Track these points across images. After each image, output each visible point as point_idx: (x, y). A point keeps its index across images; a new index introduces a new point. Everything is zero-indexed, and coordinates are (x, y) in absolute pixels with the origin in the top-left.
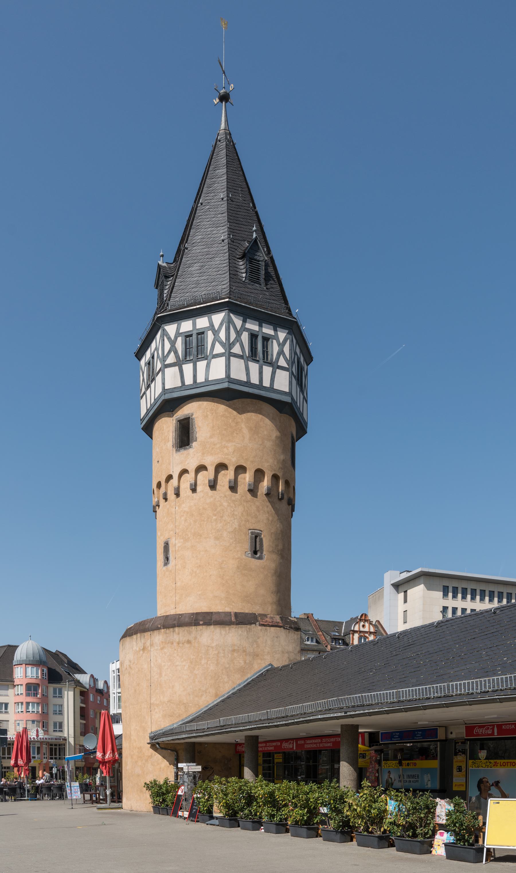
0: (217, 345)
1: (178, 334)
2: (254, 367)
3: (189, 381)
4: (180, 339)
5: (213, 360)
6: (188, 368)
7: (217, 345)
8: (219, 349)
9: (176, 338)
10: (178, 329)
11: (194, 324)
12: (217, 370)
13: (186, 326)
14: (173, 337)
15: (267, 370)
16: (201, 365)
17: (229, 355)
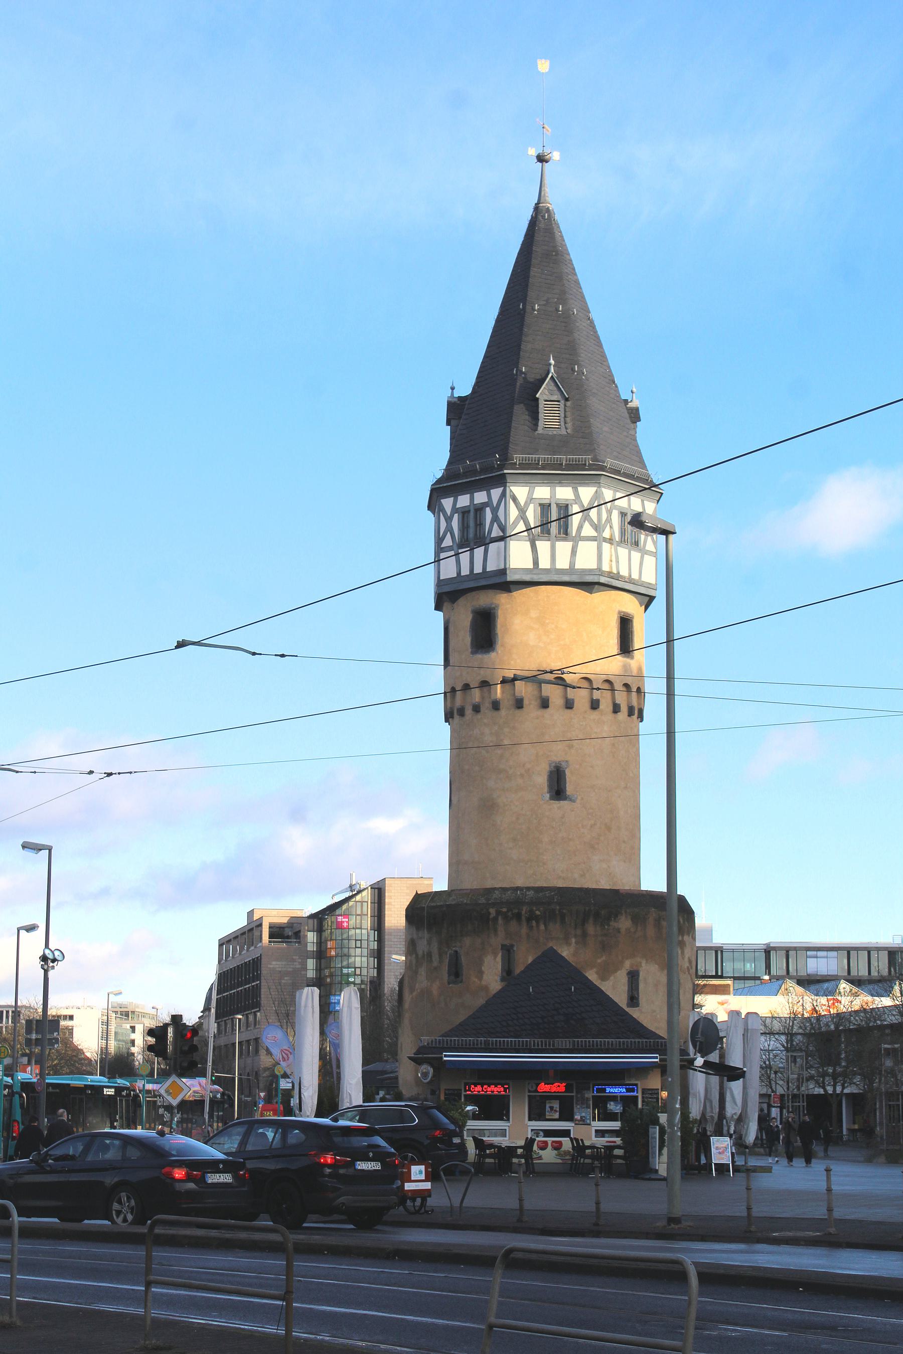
0: (587, 525)
1: (530, 500)
2: (623, 552)
3: (545, 563)
4: (531, 507)
5: (581, 544)
6: (543, 546)
7: (587, 525)
8: (588, 530)
9: (527, 504)
10: (531, 493)
11: (553, 493)
12: (587, 558)
13: (542, 492)
14: (522, 502)
15: (636, 556)
16: (564, 548)
17: (598, 539)
